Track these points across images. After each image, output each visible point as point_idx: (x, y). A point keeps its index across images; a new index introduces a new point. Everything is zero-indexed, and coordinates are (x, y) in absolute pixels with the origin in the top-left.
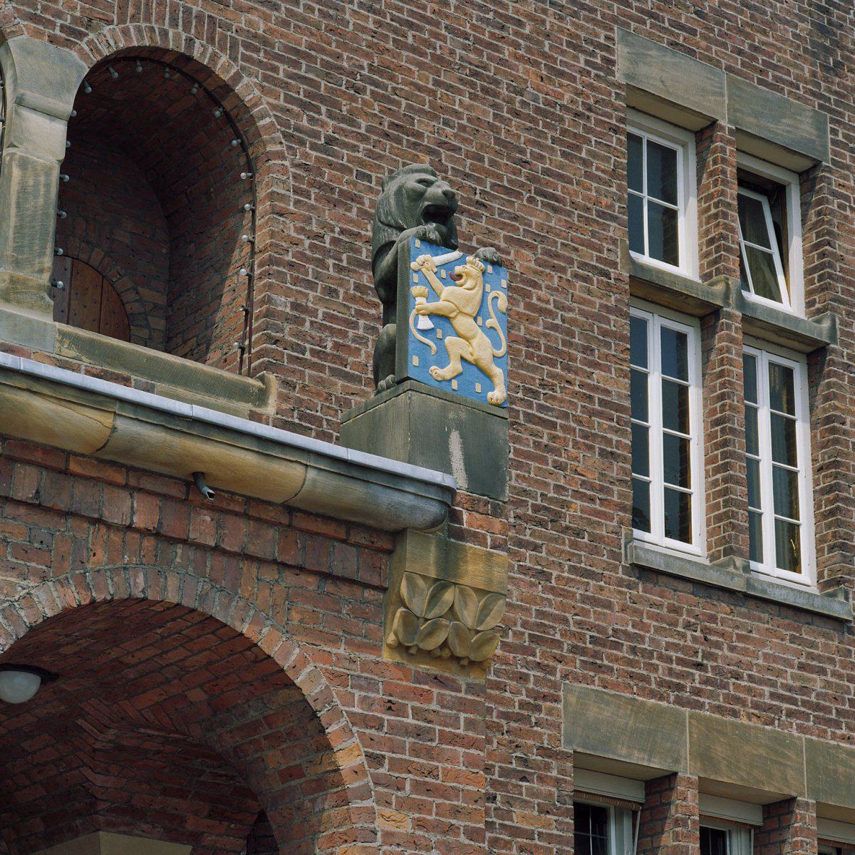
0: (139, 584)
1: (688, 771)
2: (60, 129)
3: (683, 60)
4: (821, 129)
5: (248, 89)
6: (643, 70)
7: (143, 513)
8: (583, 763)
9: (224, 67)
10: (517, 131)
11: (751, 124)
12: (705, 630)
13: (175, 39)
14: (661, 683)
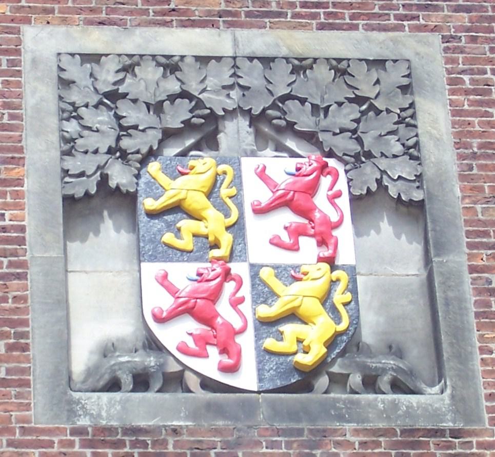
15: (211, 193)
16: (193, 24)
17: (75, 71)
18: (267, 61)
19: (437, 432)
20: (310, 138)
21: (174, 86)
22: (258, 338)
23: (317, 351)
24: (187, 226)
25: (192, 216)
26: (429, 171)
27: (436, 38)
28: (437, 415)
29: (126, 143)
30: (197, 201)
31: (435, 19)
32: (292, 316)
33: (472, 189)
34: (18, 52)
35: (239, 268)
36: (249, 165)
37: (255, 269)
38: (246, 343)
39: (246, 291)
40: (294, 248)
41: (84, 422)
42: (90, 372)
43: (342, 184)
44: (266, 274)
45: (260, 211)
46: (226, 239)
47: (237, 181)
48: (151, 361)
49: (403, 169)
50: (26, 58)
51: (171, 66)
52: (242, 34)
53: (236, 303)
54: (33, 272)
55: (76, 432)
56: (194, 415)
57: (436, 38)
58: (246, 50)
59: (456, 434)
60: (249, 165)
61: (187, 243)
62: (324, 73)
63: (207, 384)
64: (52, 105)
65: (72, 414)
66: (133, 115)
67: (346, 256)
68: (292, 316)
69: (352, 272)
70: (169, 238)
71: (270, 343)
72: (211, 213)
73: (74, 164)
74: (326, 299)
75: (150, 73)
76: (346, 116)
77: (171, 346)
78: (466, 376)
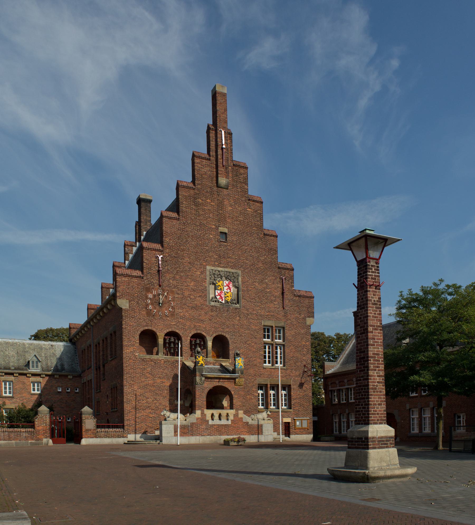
2: (211, 343)
3: (269, 321)
5: (227, 336)
6: (265, 323)
9: (224, 335)
10: (252, 333)
11: (277, 325)
13: (220, 333)
15: (222, 284)
16: (221, 267)
17: (211, 271)
19: (238, 308)
20: (230, 280)
21: (219, 273)
22: (225, 298)
23: (229, 300)
24: (220, 287)
25: (220, 286)
26: (239, 284)
27: (241, 271)
28: (238, 307)
29: (215, 279)
30: (221, 285)
31: (241, 269)
32: (228, 297)
33: (242, 286)
35: (223, 292)
36: (225, 282)
37: (225, 292)
38: (224, 298)
39: (224, 294)
40: (228, 290)
41: (211, 305)
42: (211, 300)
43: (232, 285)
44: (226, 292)
45: (225, 286)
46: (223, 289)
47: (224, 283)
48: (216, 300)
49: (237, 284)
50: (207, 269)
51: (219, 271)
52: (225, 269)
53: (223, 295)
55: (211, 306)
56: (220, 305)
57: (241, 271)
58: (225, 270)
60: (225, 282)
61: (219, 289)
62: (231, 273)
63: (221, 302)
64: (209, 274)
65: (210, 304)
66: (216, 276)
67: (232, 291)
68: (228, 297)
69: (232, 293)
70: (218, 288)
71: (226, 299)
72: (222, 286)
73: (211, 280)
74: (230, 296)
75: (217, 272)
76: (233, 278)
78: (241, 304)
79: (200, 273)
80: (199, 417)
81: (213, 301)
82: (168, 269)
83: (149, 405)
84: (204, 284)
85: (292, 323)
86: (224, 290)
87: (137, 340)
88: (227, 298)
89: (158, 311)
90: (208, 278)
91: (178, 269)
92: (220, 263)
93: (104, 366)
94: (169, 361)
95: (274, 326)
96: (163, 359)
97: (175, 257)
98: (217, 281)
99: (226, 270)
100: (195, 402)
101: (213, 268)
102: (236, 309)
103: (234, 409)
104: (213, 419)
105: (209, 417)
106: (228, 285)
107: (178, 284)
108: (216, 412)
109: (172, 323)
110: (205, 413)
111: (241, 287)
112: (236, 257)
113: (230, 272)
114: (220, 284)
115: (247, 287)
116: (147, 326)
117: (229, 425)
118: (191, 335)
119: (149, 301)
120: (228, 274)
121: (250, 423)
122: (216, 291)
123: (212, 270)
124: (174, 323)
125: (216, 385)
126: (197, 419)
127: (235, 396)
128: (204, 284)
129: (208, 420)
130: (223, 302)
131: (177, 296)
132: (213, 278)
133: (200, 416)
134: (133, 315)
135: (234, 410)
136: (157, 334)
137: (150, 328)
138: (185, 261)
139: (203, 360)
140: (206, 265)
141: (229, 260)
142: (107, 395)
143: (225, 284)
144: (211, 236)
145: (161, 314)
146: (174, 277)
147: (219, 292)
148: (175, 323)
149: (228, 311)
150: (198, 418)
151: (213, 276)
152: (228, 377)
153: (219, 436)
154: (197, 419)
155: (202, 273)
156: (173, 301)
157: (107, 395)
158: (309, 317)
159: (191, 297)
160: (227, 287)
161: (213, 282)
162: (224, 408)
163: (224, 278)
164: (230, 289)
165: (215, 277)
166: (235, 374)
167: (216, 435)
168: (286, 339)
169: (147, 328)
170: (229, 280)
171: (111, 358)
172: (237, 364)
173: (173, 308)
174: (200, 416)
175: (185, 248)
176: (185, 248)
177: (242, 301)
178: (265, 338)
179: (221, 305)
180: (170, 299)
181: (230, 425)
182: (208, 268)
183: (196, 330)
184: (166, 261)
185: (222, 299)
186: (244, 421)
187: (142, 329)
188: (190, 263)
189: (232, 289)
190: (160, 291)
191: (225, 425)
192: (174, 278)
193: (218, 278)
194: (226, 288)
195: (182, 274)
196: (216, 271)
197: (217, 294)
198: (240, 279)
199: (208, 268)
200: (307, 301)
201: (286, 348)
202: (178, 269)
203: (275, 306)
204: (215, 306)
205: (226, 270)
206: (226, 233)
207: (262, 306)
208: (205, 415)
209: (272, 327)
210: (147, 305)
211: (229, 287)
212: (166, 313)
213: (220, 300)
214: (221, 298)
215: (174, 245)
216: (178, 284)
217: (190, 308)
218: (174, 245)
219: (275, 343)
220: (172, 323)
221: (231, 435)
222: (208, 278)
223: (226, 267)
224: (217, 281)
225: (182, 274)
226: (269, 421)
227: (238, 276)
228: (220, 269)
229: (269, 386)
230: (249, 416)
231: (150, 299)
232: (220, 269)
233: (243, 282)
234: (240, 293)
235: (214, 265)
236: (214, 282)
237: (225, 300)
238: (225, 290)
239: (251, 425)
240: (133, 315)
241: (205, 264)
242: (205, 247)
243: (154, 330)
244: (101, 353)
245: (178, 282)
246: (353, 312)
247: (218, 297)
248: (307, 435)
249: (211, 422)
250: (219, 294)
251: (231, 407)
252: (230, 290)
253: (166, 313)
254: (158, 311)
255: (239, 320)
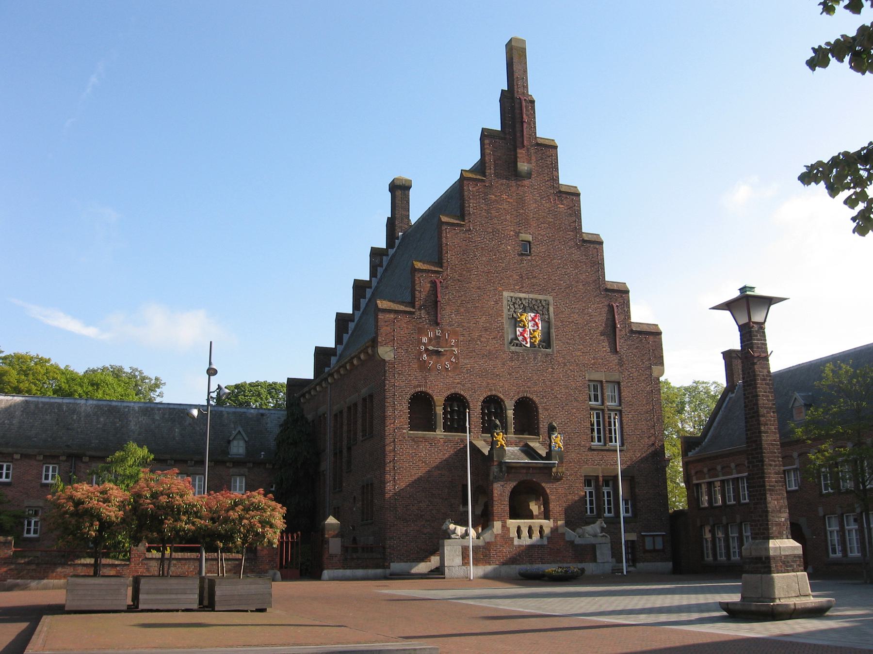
0: (525, 478)
1: (601, 475)
4: (620, 376)
5: (535, 398)
7: (524, 471)
8: (585, 476)
11: (608, 380)
12: (603, 456)
14: (596, 464)
18: (532, 299)
27: (552, 297)
34: (502, 296)
36: (529, 314)
37: (530, 330)
38: (528, 340)
39: (529, 333)
40: (534, 327)
45: (530, 321)
51: (521, 299)
53: (527, 334)
54: (505, 329)
55: (510, 352)
57: (552, 297)
58: (529, 297)
59: (552, 355)
63: (524, 346)
71: (532, 341)
77: (520, 340)
78: (553, 347)
79: (493, 303)
80: (498, 533)
81: (513, 345)
82: (449, 299)
83: (422, 514)
84: (500, 319)
85: (631, 375)
86: (528, 328)
87: (405, 409)
88: (534, 339)
89: (436, 363)
90: (505, 311)
91: (463, 298)
92: (522, 287)
93: (349, 449)
94: (450, 441)
95: (604, 381)
96: (443, 437)
97: (459, 280)
98: (519, 314)
99: (531, 296)
100: (493, 507)
101: (512, 294)
102: (547, 355)
103: (551, 519)
104: (519, 537)
105: (513, 533)
106: (533, 319)
107: (463, 321)
108: (524, 523)
109: (455, 381)
110: (508, 526)
111: (553, 321)
112: (545, 277)
113: (536, 300)
114: (523, 318)
115: (562, 322)
116: (420, 386)
117: (545, 545)
118: (482, 399)
119: (422, 347)
120: (534, 302)
121: (576, 542)
122: (517, 329)
123: (512, 297)
124: (458, 381)
125: (522, 479)
126: (496, 537)
127: (552, 497)
128: (500, 319)
129: (513, 538)
130: (528, 345)
131: (461, 338)
132: (512, 310)
133: (500, 532)
134: (400, 370)
135: (552, 520)
136: (433, 398)
137: (423, 389)
138: (472, 286)
139: (504, 439)
140: (503, 290)
141: (535, 281)
142: (355, 497)
143: (530, 318)
144: (509, 247)
145: (439, 368)
146: (457, 311)
147: (521, 329)
148: (459, 381)
149: (535, 358)
150: (497, 534)
151: (512, 307)
152: (542, 465)
153: (529, 565)
154: (496, 536)
155: (496, 302)
156: (457, 346)
157: (355, 497)
158: (656, 364)
159: (482, 339)
160: (533, 322)
161: (513, 315)
162: (534, 517)
163: (527, 310)
164: (537, 324)
165: (515, 309)
166: (552, 460)
167: (525, 564)
168: (623, 401)
169: (419, 389)
170: (535, 312)
171: (363, 436)
172: (554, 443)
173: (456, 357)
174: (500, 532)
175: (472, 266)
176: (472, 266)
177: (555, 343)
178: (590, 401)
179: (526, 350)
180: (452, 344)
181: (546, 545)
182: (506, 294)
183: (491, 390)
184: (447, 288)
185: (526, 341)
186: (567, 539)
187: (413, 391)
188: (479, 288)
189: (540, 325)
190: (438, 333)
191: (538, 545)
192: (458, 312)
193: (520, 309)
194: (531, 324)
195: (469, 306)
196: (516, 299)
197: (518, 333)
198: (551, 309)
199: (506, 294)
200: (651, 339)
201: (623, 414)
202: (463, 298)
203: (604, 349)
204: (516, 352)
205: (531, 296)
206: (529, 242)
207: (586, 351)
208: (508, 529)
209: (601, 382)
210: (421, 354)
211: (535, 322)
212: (447, 366)
213: (524, 343)
214: (525, 339)
215: (457, 263)
216: (463, 321)
217: (480, 356)
218: (457, 263)
219: (607, 407)
220: (455, 381)
221: (548, 563)
222: (505, 311)
223: (531, 292)
224: (519, 314)
225: (469, 306)
226: (604, 538)
227: (548, 305)
228: (522, 295)
229: (601, 479)
230: (574, 530)
231: (424, 344)
232: (522, 295)
233: (556, 314)
234: (553, 331)
235: (513, 291)
236: (515, 315)
237: (530, 341)
238: (530, 328)
239: (578, 545)
240: (400, 370)
241: (500, 289)
242: (501, 264)
243: (430, 391)
244: (345, 428)
245: (462, 317)
246: (722, 353)
247: (520, 338)
248: (664, 564)
249: (516, 542)
250: (521, 333)
251: (547, 516)
252: (538, 326)
253: (447, 366)
254: (436, 363)
255: (552, 373)
